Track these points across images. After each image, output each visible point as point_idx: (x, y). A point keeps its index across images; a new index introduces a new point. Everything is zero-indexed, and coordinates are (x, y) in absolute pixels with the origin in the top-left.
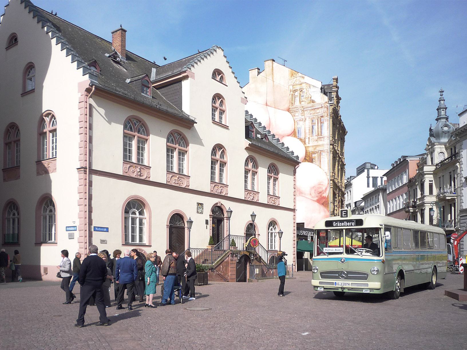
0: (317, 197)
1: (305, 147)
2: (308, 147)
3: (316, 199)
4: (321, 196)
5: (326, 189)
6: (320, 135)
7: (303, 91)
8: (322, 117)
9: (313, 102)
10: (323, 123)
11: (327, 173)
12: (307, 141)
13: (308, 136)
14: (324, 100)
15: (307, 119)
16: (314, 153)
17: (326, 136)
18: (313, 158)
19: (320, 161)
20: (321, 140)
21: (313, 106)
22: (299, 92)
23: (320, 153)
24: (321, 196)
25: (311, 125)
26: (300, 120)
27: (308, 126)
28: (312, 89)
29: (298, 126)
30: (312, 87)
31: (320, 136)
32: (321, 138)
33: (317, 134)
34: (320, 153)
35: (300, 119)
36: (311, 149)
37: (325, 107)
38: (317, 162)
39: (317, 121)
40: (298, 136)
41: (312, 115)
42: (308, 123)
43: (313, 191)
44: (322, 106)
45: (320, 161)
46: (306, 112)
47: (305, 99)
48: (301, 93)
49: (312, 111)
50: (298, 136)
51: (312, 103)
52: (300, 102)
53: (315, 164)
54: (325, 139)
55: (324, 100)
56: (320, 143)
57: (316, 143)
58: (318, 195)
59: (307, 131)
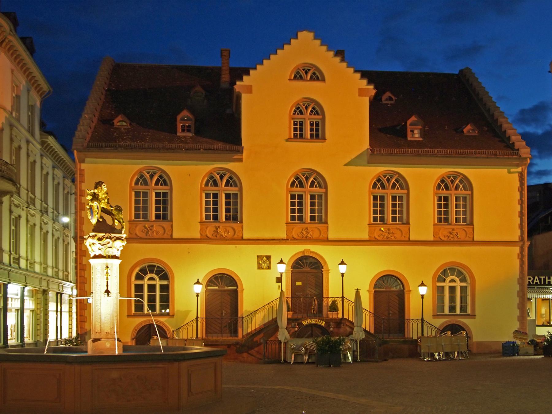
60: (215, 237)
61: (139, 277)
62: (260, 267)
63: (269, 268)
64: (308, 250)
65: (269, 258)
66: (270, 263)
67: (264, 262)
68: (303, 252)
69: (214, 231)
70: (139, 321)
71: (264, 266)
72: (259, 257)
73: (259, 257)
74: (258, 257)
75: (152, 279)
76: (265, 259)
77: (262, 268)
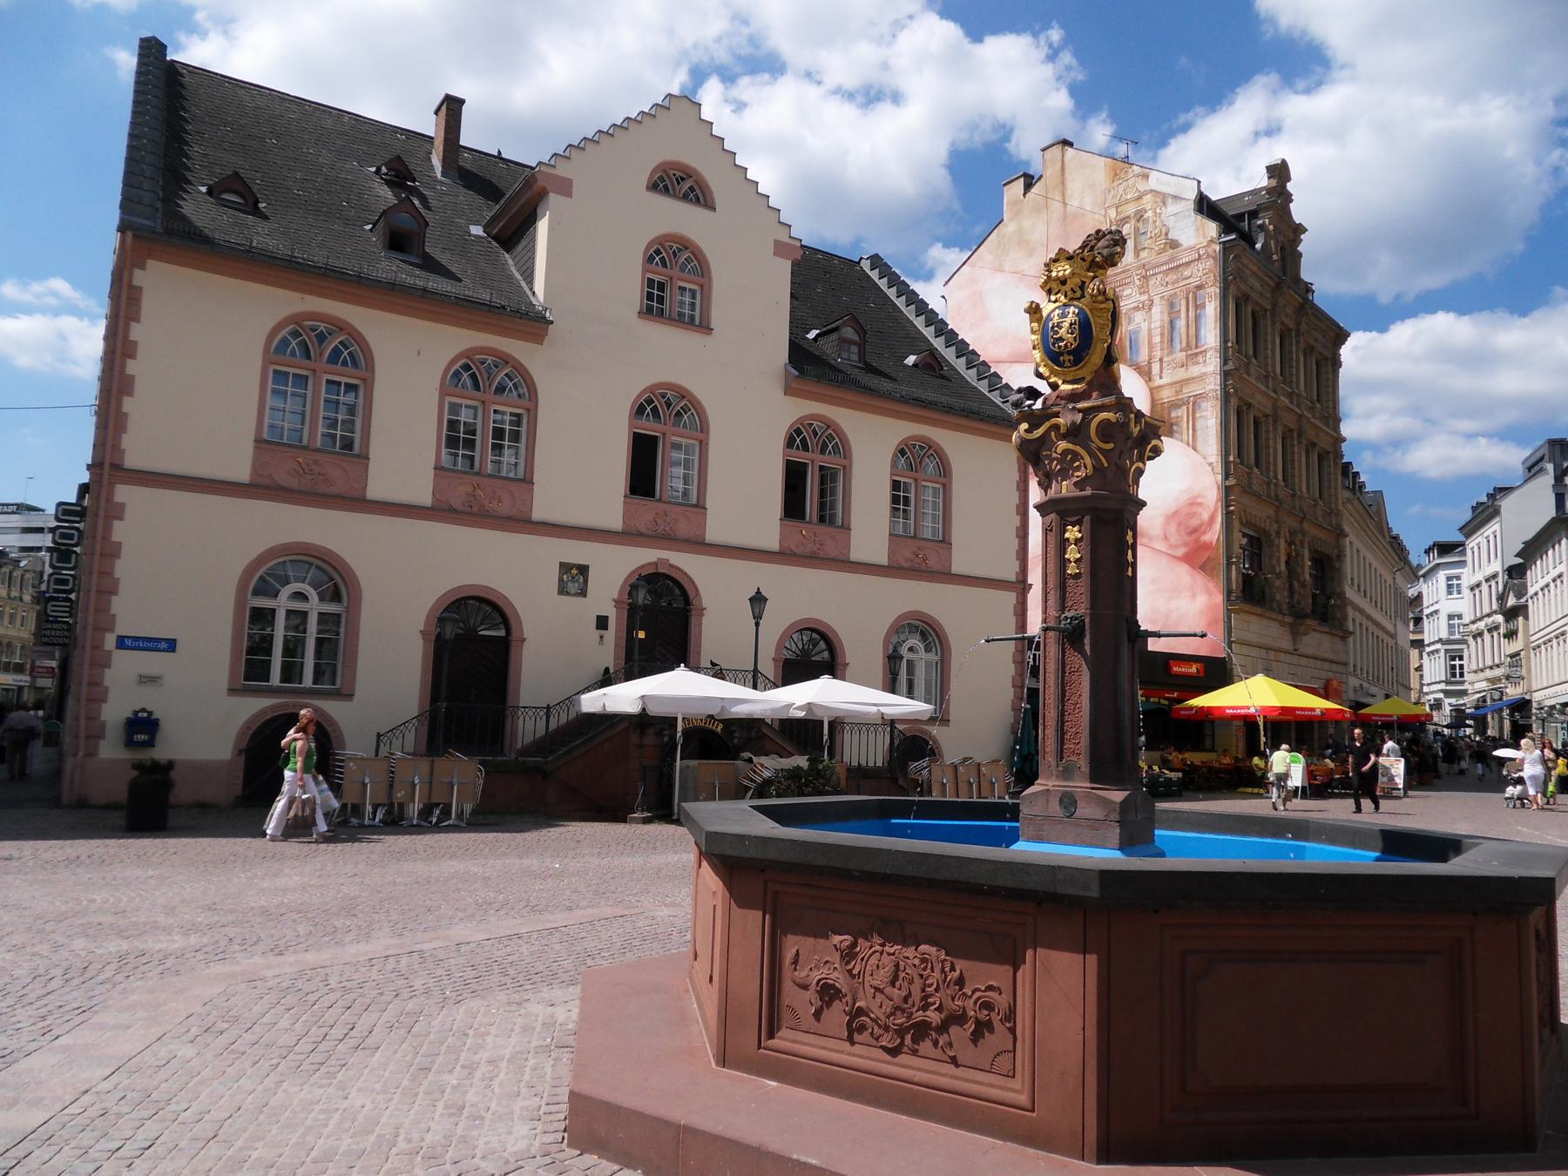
0: (1185, 544)
1: (1151, 390)
2: (1159, 387)
3: (1181, 552)
4: (1197, 541)
5: (1212, 518)
6: (1193, 347)
7: (1146, 216)
8: (1200, 287)
9: (1174, 244)
10: (1203, 306)
11: (1215, 464)
12: (1156, 368)
13: (1158, 354)
14: (1204, 234)
15: (1157, 300)
16: (1175, 405)
17: (1211, 348)
18: (1174, 421)
19: (1194, 430)
20: (1198, 363)
21: (1172, 259)
22: (1133, 222)
23: (1195, 403)
24: (1197, 541)
25: (1166, 319)
26: (1134, 308)
27: (1158, 324)
28: (1172, 208)
29: (1130, 328)
30: (1170, 201)
31: (1193, 350)
32: (1196, 354)
33: (1184, 345)
34: (1194, 403)
35: (1135, 305)
36: (1166, 395)
37: (1208, 256)
38: (1185, 432)
39: (1183, 302)
40: (1131, 359)
41: (1170, 287)
42: (1158, 313)
43: (1173, 528)
44: (1199, 256)
45: (1194, 430)
46: (1151, 282)
47: (1150, 241)
48: (1140, 225)
49: (1170, 276)
50: (1131, 359)
51: (1171, 251)
52: (1137, 252)
53: (1177, 439)
54: (1208, 356)
55: (1204, 234)
56: (1195, 370)
57: (1181, 374)
58: (1188, 539)
59: (1157, 339)
60: (469, 510)
62: (562, 591)
63: (583, 593)
64: (664, 562)
65: (583, 570)
66: (586, 581)
67: (573, 578)
68: (655, 564)
69: (467, 494)
70: (253, 706)
71: (573, 587)
72: (565, 567)
73: (565, 567)
74: (562, 565)
76: (574, 571)
77: (568, 594)
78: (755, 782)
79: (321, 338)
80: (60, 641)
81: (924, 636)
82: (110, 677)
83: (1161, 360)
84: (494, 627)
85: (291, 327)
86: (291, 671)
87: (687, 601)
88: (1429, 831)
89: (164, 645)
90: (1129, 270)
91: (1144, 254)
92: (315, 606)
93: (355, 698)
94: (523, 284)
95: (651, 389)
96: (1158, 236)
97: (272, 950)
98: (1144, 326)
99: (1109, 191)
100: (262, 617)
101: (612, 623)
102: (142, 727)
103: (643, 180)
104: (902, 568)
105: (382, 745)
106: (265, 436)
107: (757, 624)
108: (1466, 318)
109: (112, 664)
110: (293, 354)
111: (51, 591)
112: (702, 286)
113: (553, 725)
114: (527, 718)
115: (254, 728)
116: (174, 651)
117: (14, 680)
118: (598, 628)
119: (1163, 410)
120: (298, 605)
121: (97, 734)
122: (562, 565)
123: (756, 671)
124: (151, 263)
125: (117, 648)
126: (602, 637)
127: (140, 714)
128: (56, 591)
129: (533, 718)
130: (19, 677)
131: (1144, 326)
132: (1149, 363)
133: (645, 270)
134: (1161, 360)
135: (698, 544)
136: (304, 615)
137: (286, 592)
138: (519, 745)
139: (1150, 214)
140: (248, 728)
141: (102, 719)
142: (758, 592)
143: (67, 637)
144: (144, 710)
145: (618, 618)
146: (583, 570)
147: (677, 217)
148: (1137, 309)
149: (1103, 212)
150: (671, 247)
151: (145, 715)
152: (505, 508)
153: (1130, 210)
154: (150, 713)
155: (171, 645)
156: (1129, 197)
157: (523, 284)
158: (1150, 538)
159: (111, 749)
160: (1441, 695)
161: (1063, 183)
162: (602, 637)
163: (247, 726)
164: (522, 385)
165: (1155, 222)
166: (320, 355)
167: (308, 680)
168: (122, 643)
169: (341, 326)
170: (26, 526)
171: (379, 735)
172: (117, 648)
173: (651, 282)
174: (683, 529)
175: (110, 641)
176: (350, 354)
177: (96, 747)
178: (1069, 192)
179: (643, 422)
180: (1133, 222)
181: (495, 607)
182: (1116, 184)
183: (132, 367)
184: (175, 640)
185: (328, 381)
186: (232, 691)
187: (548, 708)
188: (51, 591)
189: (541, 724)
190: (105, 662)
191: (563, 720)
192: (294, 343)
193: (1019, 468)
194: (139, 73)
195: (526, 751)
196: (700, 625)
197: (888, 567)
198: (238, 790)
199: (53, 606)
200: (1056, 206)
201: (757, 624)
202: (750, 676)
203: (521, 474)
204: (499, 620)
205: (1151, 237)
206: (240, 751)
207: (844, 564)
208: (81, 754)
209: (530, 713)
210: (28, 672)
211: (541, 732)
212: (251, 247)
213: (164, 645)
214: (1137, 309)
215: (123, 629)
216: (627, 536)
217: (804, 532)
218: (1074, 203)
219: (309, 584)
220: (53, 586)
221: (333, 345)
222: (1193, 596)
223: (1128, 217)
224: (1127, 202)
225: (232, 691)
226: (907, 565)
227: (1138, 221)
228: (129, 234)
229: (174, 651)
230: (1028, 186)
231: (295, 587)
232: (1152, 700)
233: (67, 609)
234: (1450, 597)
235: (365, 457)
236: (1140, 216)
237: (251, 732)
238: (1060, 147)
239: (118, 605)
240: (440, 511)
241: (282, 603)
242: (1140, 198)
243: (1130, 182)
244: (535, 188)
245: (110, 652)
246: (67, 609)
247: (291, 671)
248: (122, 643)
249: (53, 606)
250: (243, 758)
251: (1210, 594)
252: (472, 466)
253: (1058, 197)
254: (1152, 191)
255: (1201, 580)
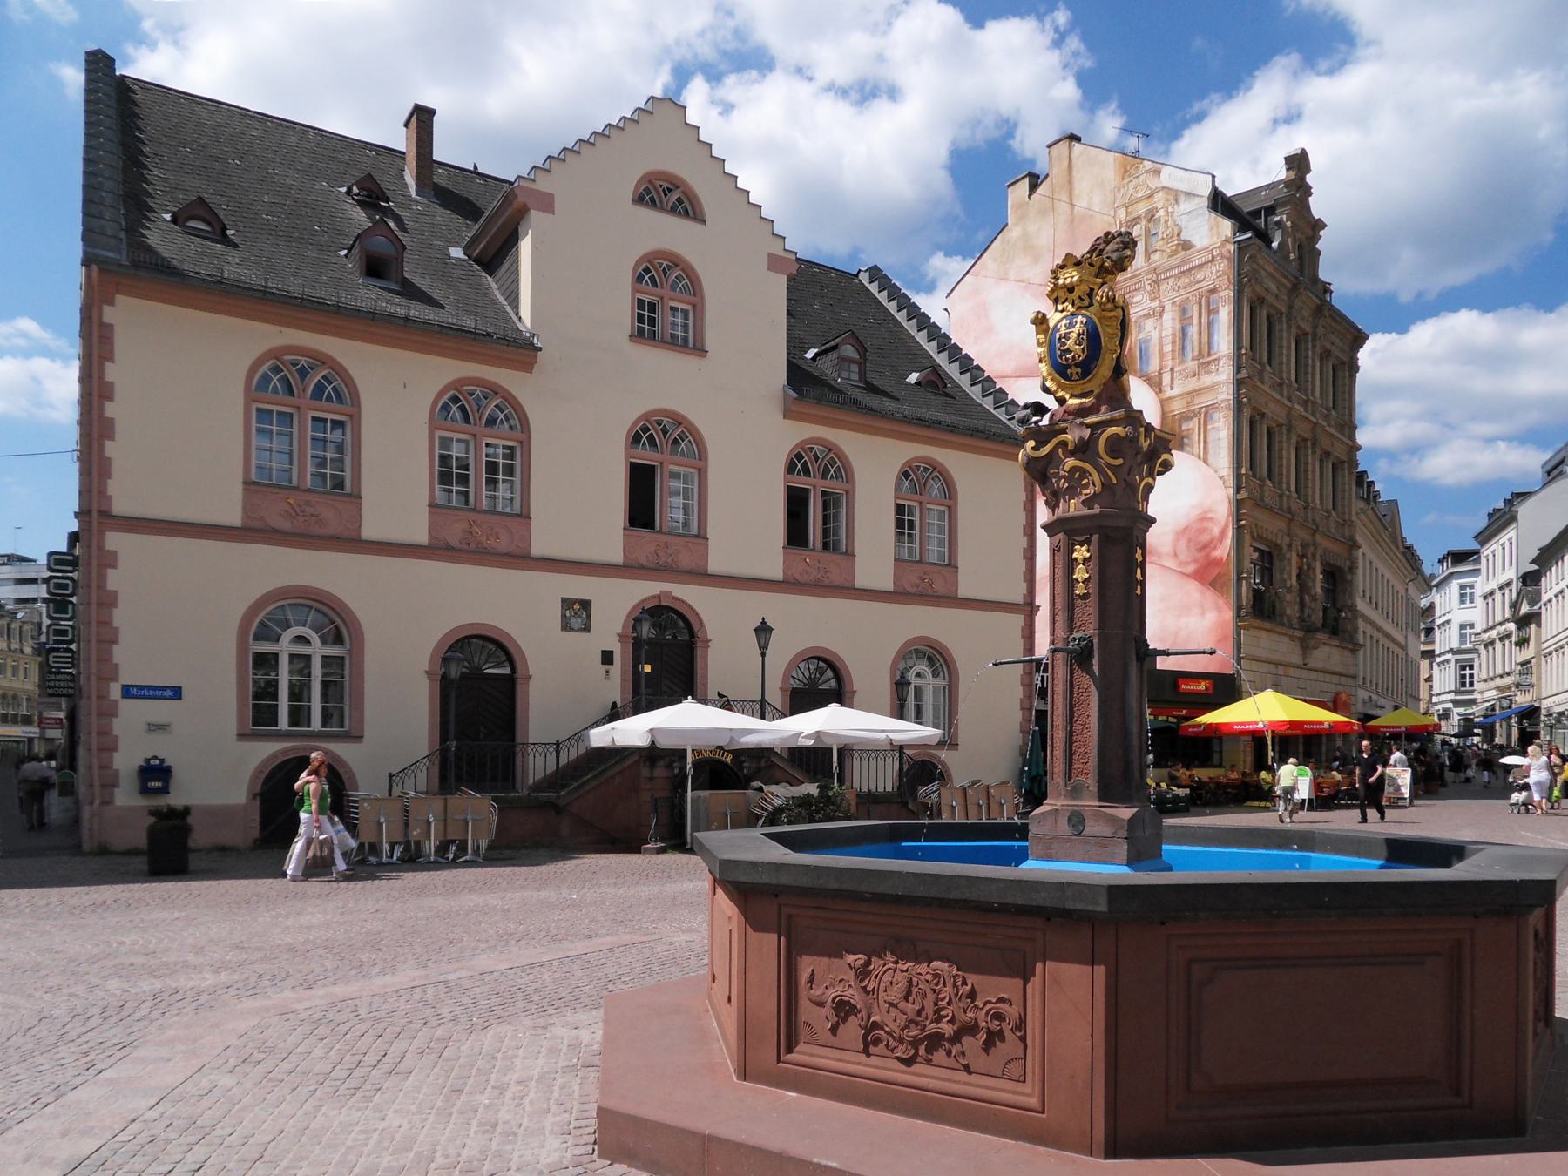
0: (1195, 561)
1: (1162, 401)
2: (1170, 398)
3: (1191, 568)
4: (1207, 556)
5: (1223, 533)
6: (1206, 355)
7: (1158, 215)
8: (1213, 291)
9: (1186, 246)
10: (1216, 311)
11: (1226, 478)
12: (1166, 379)
13: (1169, 363)
14: (1218, 233)
15: (1168, 307)
16: (1186, 417)
17: (1224, 356)
18: (1185, 433)
19: (1205, 442)
20: (1209, 372)
21: (1185, 262)
22: (1144, 222)
23: (1207, 414)
24: (1207, 556)
25: (1178, 326)
26: (1145, 315)
27: (1170, 331)
28: (1185, 206)
29: (1140, 336)
30: (1182, 198)
31: (1206, 358)
32: (1209, 363)
33: (1196, 353)
34: (1206, 414)
35: (1146, 312)
36: (1177, 407)
37: (1222, 257)
38: (1196, 445)
39: (1196, 308)
40: (1141, 369)
41: (1182, 292)
42: (1170, 320)
43: (1183, 544)
44: (1213, 256)
45: (1205, 442)
46: (1163, 287)
47: (1161, 243)
48: (1151, 225)
49: (1183, 279)
50: (1141, 369)
51: (1183, 253)
52: (1148, 255)
53: (1188, 452)
54: (1221, 364)
55: (1218, 233)
56: (1207, 380)
57: (1192, 384)
58: (1198, 555)
59: (1168, 348)
60: (466, 547)
61: (265, 634)
62: (566, 627)
63: (586, 628)
64: (668, 594)
65: (586, 605)
66: (589, 617)
67: (576, 613)
69: (464, 531)
70: (266, 751)
71: (576, 623)
72: (567, 603)
73: (567, 603)
74: (564, 600)
75: (301, 640)
76: (577, 607)
77: (572, 629)
78: (766, 810)
79: (303, 373)
80: (65, 692)
81: (931, 661)
82: (118, 726)
83: (1172, 370)
84: (499, 665)
85: (272, 362)
86: (299, 715)
87: (692, 634)
88: (1433, 839)
89: (169, 693)
90: (1139, 275)
91: (1155, 257)
92: (318, 650)
93: (365, 740)
94: (508, 309)
95: (646, 416)
96: (1166, 239)
97: (301, 984)
98: (1155, 334)
99: (1119, 189)
100: (266, 662)
101: (617, 657)
102: (155, 774)
103: (630, 195)
104: (909, 594)
105: (394, 785)
106: (254, 478)
107: (763, 655)
108: (1490, 316)
109: (120, 713)
110: (275, 390)
111: (51, 642)
112: (694, 306)
113: (563, 761)
114: (537, 754)
115: (267, 772)
116: (180, 698)
117: (23, 732)
118: (603, 663)
119: (1173, 422)
120: (301, 649)
121: (111, 783)
122: (564, 600)
123: (763, 701)
124: (120, 299)
125: (123, 697)
126: (607, 672)
127: (152, 762)
128: (56, 642)
129: (543, 755)
130: (28, 729)
131: (1155, 334)
132: (1160, 374)
133: (634, 291)
134: (1172, 370)
135: (701, 576)
136: (307, 659)
137: (288, 635)
138: (531, 781)
139: (1161, 213)
140: (261, 772)
141: (115, 767)
142: (763, 622)
143: (71, 688)
144: (155, 758)
145: (623, 652)
146: (586, 605)
147: (666, 233)
148: (1147, 316)
149: (1112, 213)
150: (661, 265)
151: (157, 762)
152: (503, 544)
153: (1141, 209)
154: (162, 761)
155: (177, 693)
156: (1140, 195)
157: (508, 309)
158: (1160, 556)
159: (126, 797)
160: (1450, 705)
161: (1070, 182)
162: (607, 672)
163: (259, 771)
164: (513, 416)
165: (1166, 222)
166: (304, 391)
167: (316, 723)
168: (127, 691)
169: (323, 360)
170: (19, 577)
171: (391, 776)
172: (123, 697)
173: (641, 303)
174: (685, 561)
175: (115, 691)
176: (334, 389)
177: (112, 795)
178: (1076, 192)
179: (639, 451)
180: (1144, 222)
181: (499, 645)
182: (1126, 181)
183: (110, 409)
184: (180, 688)
185: (314, 419)
186: (242, 736)
187: (558, 744)
188: (51, 642)
189: (552, 760)
190: (111, 711)
191: (573, 755)
192: (275, 380)
193: (1026, 487)
194: (88, 91)
195: (538, 787)
196: (705, 658)
197: (894, 593)
198: (255, 833)
199: (54, 657)
200: (1063, 207)
201: (763, 655)
202: (758, 706)
203: (517, 509)
204: (504, 658)
205: (1163, 239)
206: (255, 796)
207: (848, 590)
208: (97, 802)
209: (540, 749)
210: (36, 724)
211: (552, 768)
212: (223, 278)
213: (169, 693)
214: (1147, 316)
215: (127, 678)
216: (629, 569)
217: (808, 560)
218: (1082, 203)
219: (309, 628)
220: (52, 638)
221: (316, 380)
222: (1203, 613)
223: (1139, 217)
224: (1138, 201)
225: (242, 736)
226: (913, 590)
227: (1149, 221)
228: (94, 268)
229: (180, 698)
230: (1033, 187)
231: (297, 630)
232: (1160, 718)
233: (70, 660)
234: (1462, 606)
235: (357, 497)
236: (1151, 216)
237: (263, 776)
238: (1066, 142)
239: (119, 654)
240: (437, 550)
241: (284, 648)
242: (1151, 196)
243: (1142, 178)
244: (515, 205)
245: (116, 702)
246: (70, 660)
247: (299, 715)
248: (127, 691)
249: (54, 657)
250: (257, 803)
251: (1219, 610)
252: (467, 502)
253: (1065, 198)
254: (1163, 188)
255: (1210, 596)
